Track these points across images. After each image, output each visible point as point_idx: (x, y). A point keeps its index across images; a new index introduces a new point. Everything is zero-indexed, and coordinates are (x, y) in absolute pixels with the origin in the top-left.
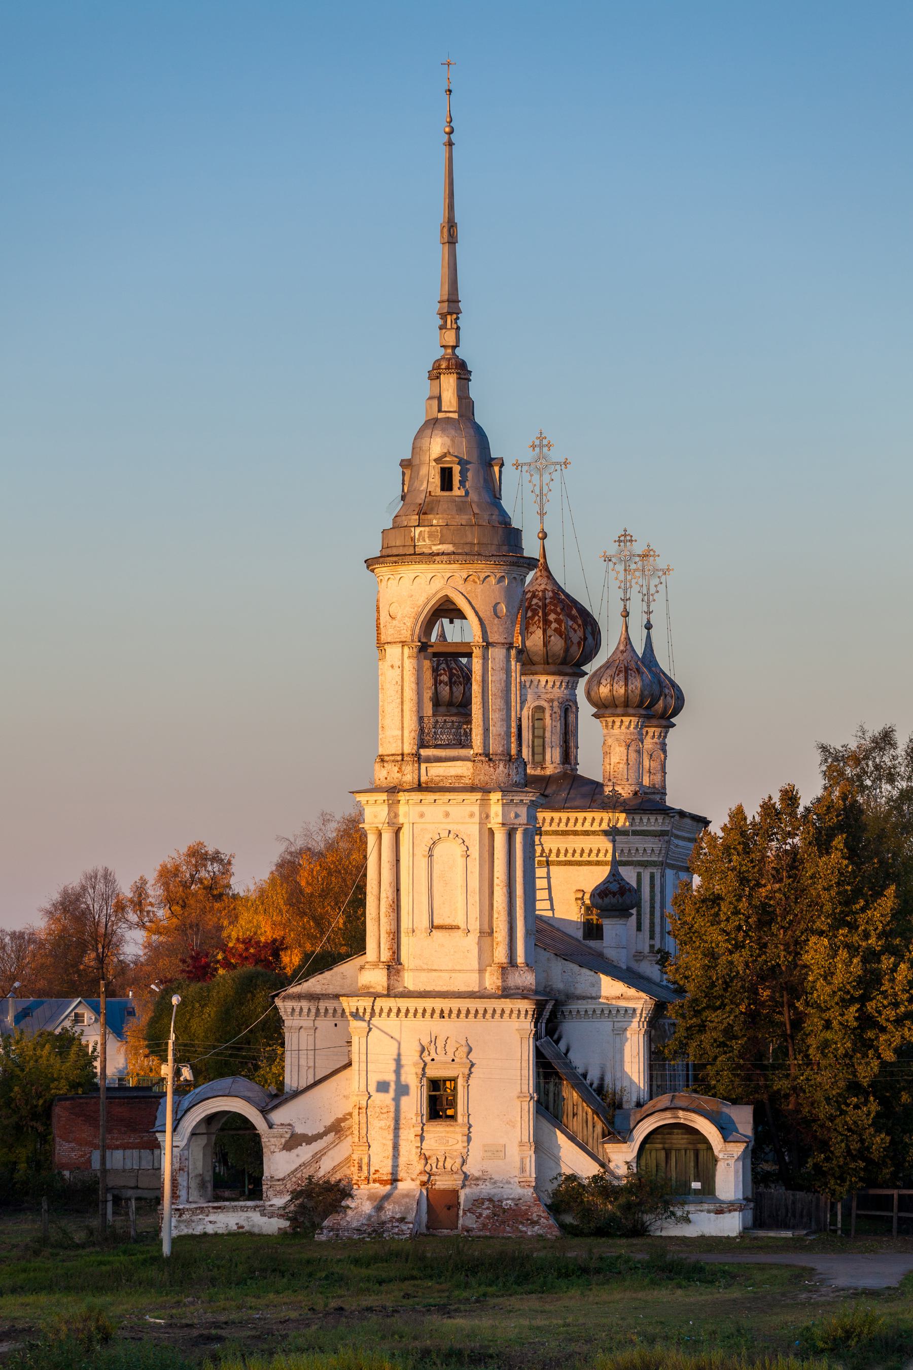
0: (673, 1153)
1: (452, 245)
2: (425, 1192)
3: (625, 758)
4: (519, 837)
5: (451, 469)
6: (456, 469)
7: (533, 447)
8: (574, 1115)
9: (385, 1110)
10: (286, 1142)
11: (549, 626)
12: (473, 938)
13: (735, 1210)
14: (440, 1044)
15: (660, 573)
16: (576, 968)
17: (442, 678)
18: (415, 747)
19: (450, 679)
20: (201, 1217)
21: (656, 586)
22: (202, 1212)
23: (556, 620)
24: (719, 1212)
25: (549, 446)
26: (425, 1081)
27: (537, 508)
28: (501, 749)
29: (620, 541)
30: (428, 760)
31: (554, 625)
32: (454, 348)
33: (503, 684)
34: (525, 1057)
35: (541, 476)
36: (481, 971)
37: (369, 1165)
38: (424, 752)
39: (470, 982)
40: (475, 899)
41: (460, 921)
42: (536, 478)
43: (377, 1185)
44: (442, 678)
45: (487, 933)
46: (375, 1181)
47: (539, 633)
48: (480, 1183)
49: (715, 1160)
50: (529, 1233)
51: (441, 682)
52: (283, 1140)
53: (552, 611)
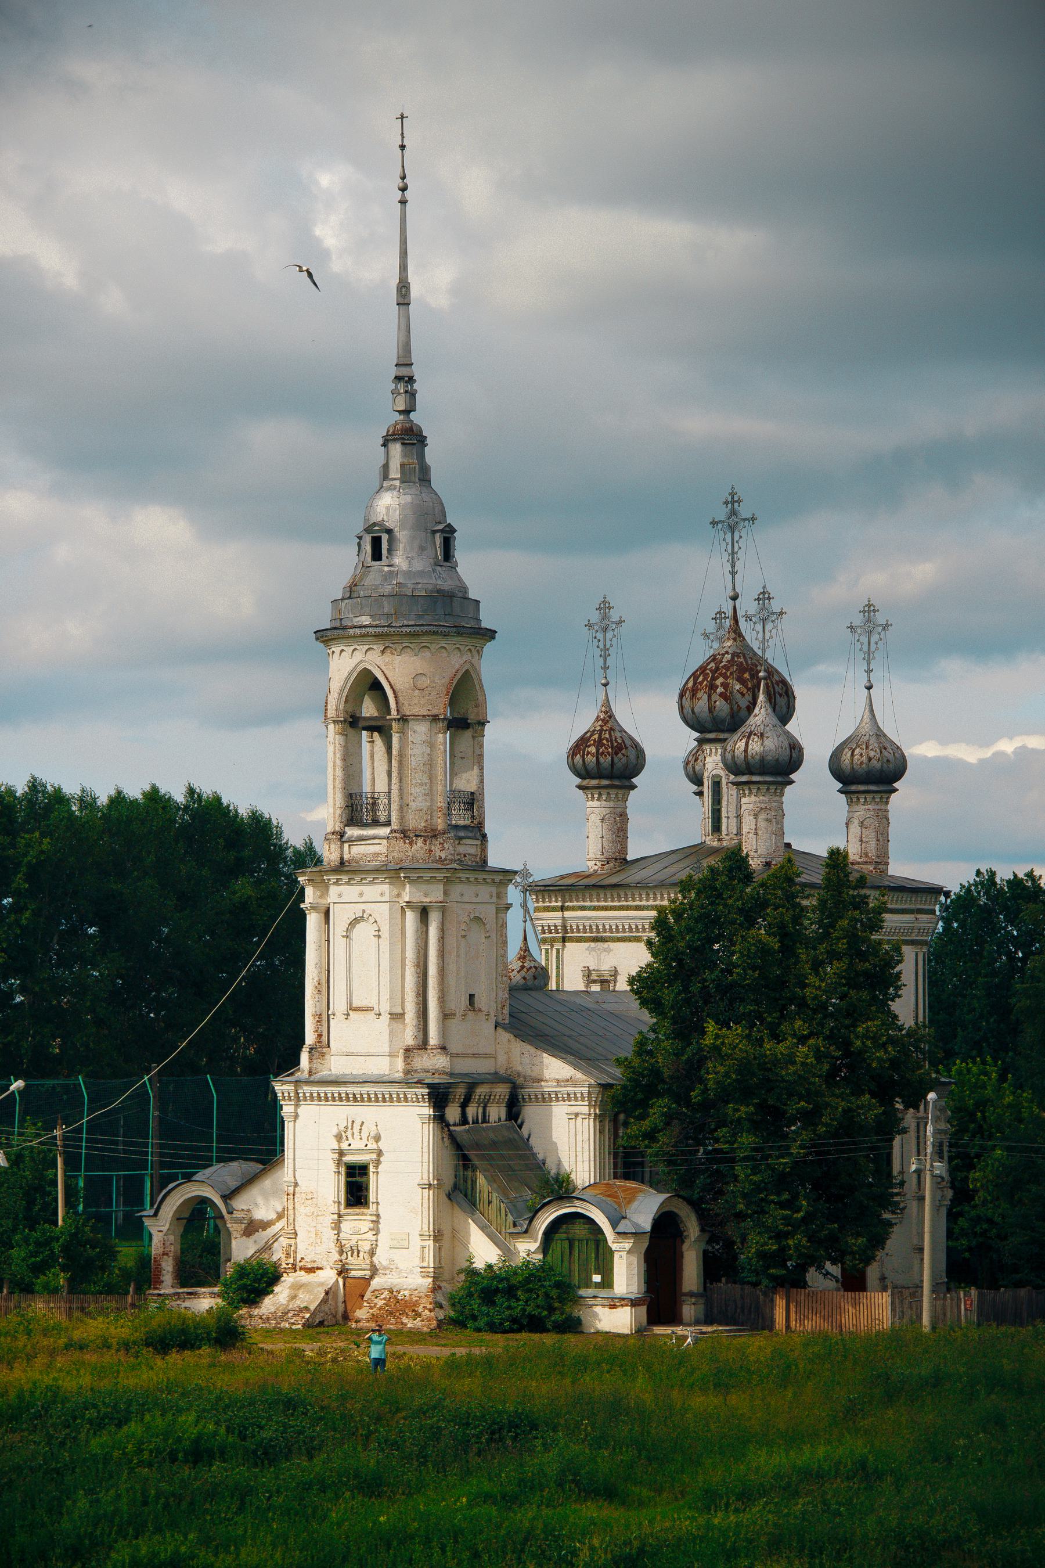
0: (576, 1244)
1: (405, 307)
2: (341, 1281)
3: (753, 827)
5: (380, 538)
6: (385, 537)
7: (726, 503)
8: (490, 1203)
9: (310, 1197)
10: (246, 1228)
11: (715, 691)
12: (385, 1018)
13: (627, 1305)
14: (357, 1127)
15: (880, 629)
16: (532, 1050)
17: (590, 749)
18: (342, 825)
19: (597, 751)
20: (178, 1302)
21: (876, 643)
22: (179, 1298)
23: (722, 684)
24: (613, 1307)
25: (739, 501)
26: (343, 1170)
27: (728, 567)
28: (423, 824)
29: (759, 599)
31: (720, 690)
32: (406, 412)
33: (426, 758)
34: (426, 1144)
35: (733, 534)
37: (295, 1252)
40: (385, 978)
41: (372, 1002)
42: (729, 535)
43: (303, 1273)
44: (590, 749)
46: (301, 1269)
47: (706, 697)
48: (388, 1272)
49: (611, 1253)
50: (409, 1325)
51: (589, 753)
52: (243, 1226)
53: (721, 675)
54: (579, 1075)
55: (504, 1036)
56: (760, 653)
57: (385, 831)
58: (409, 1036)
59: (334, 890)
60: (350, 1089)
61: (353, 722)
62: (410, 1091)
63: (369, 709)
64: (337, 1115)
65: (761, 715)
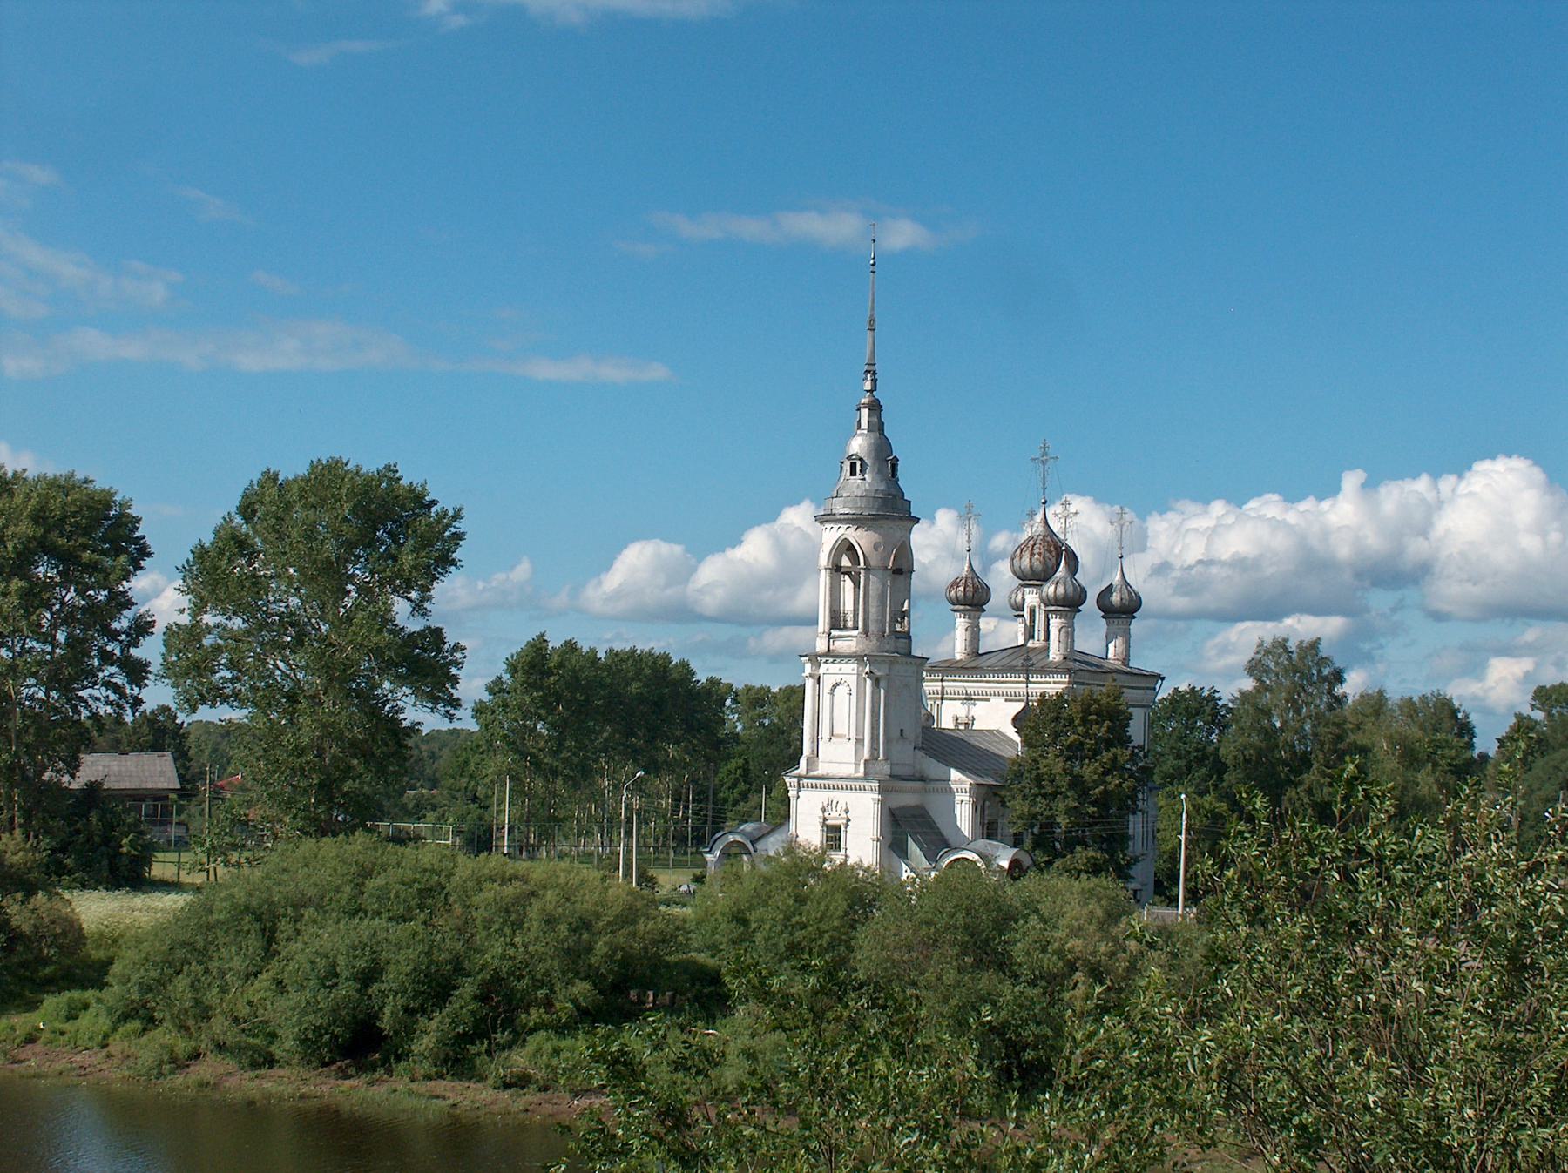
4: (883, 683)
30: (835, 638)
36: (857, 764)
38: (835, 633)
39: (849, 770)
45: (859, 742)
54: (964, 778)
55: (920, 754)
56: (1062, 537)
57: (855, 633)
58: (866, 755)
59: (824, 667)
60: (831, 782)
61: (836, 569)
62: (867, 784)
63: (846, 562)
64: (822, 797)
65: (1062, 571)
